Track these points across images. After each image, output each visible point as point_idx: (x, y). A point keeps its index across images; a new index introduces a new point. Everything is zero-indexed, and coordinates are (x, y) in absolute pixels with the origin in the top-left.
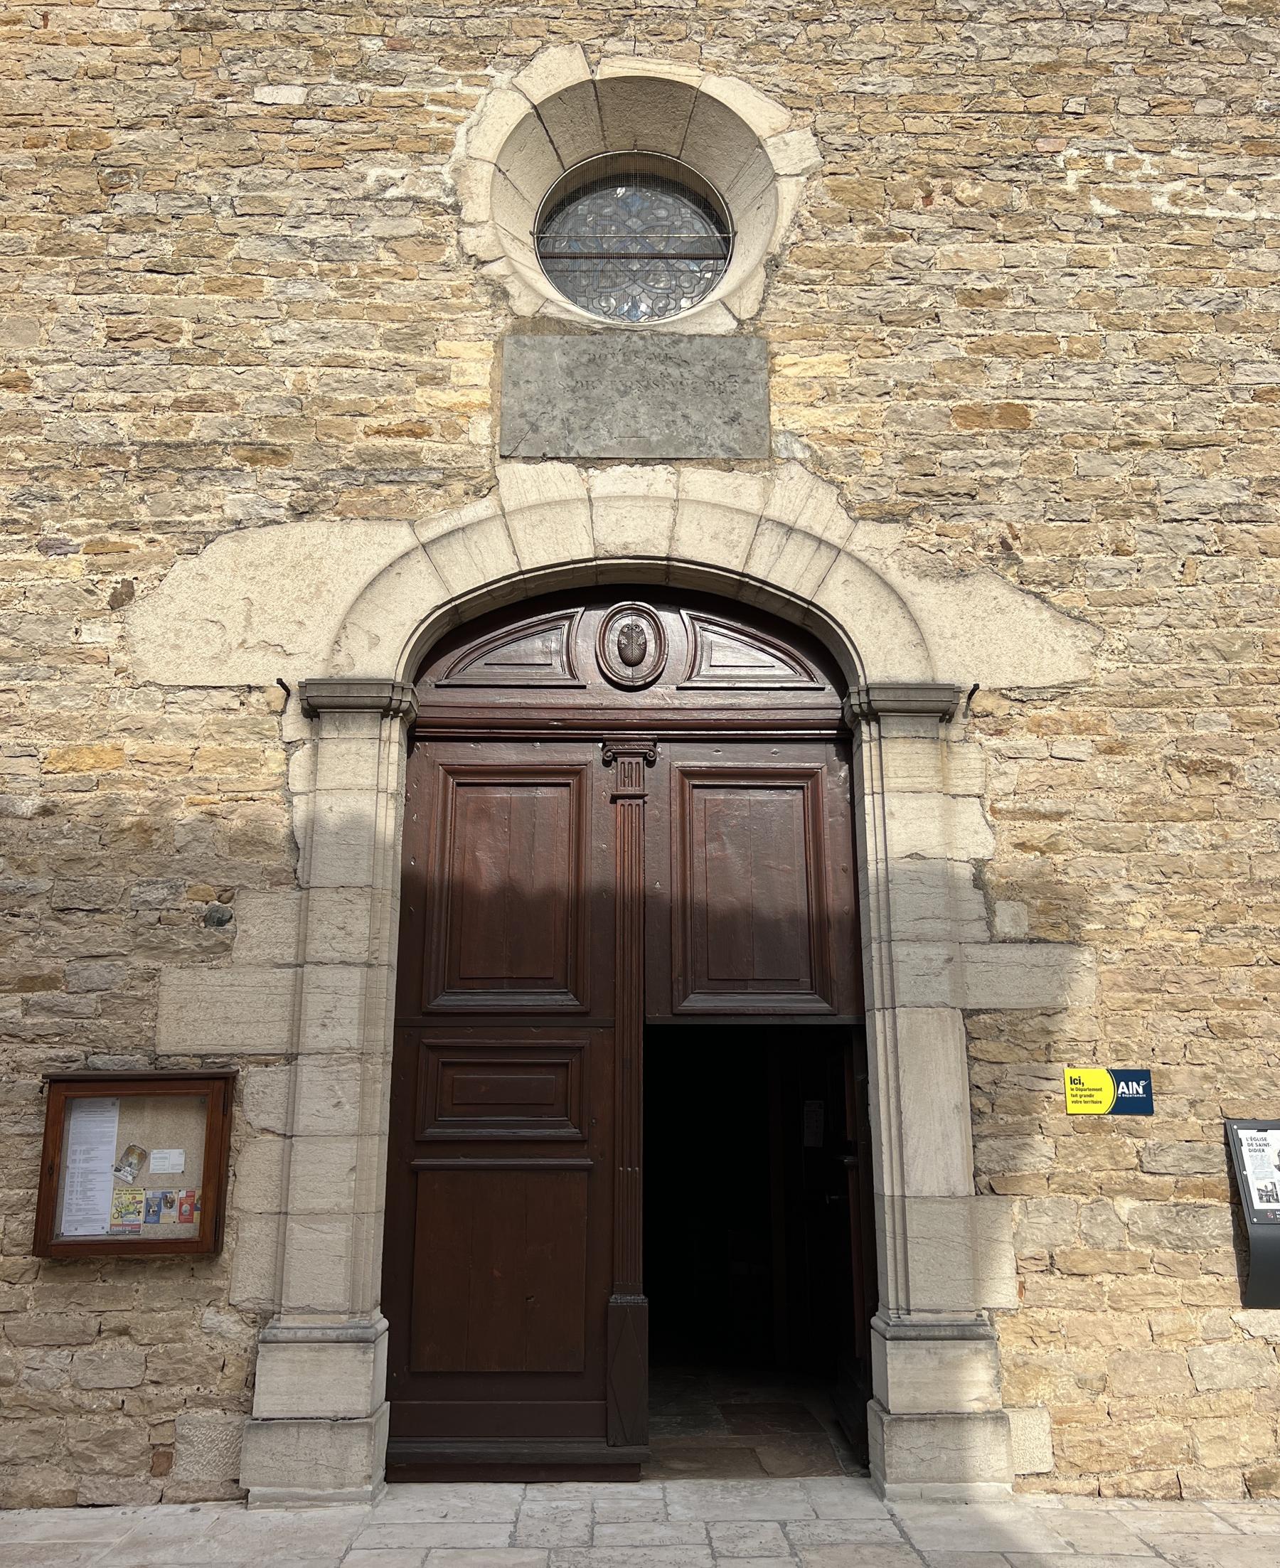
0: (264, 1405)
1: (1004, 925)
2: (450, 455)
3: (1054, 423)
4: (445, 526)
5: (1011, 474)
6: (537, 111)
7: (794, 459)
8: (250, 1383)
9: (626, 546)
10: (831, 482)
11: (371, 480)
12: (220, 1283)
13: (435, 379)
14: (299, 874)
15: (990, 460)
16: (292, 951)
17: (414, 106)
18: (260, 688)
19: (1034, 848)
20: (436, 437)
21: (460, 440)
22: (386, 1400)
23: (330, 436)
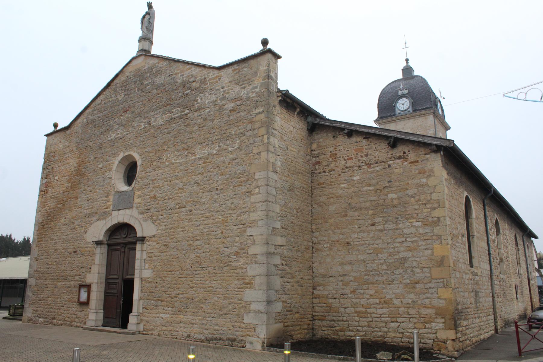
0: (89, 318)
1: (146, 267)
3: (158, 198)
6: (119, 162)
13: (108, 201)
17: (109, 165)
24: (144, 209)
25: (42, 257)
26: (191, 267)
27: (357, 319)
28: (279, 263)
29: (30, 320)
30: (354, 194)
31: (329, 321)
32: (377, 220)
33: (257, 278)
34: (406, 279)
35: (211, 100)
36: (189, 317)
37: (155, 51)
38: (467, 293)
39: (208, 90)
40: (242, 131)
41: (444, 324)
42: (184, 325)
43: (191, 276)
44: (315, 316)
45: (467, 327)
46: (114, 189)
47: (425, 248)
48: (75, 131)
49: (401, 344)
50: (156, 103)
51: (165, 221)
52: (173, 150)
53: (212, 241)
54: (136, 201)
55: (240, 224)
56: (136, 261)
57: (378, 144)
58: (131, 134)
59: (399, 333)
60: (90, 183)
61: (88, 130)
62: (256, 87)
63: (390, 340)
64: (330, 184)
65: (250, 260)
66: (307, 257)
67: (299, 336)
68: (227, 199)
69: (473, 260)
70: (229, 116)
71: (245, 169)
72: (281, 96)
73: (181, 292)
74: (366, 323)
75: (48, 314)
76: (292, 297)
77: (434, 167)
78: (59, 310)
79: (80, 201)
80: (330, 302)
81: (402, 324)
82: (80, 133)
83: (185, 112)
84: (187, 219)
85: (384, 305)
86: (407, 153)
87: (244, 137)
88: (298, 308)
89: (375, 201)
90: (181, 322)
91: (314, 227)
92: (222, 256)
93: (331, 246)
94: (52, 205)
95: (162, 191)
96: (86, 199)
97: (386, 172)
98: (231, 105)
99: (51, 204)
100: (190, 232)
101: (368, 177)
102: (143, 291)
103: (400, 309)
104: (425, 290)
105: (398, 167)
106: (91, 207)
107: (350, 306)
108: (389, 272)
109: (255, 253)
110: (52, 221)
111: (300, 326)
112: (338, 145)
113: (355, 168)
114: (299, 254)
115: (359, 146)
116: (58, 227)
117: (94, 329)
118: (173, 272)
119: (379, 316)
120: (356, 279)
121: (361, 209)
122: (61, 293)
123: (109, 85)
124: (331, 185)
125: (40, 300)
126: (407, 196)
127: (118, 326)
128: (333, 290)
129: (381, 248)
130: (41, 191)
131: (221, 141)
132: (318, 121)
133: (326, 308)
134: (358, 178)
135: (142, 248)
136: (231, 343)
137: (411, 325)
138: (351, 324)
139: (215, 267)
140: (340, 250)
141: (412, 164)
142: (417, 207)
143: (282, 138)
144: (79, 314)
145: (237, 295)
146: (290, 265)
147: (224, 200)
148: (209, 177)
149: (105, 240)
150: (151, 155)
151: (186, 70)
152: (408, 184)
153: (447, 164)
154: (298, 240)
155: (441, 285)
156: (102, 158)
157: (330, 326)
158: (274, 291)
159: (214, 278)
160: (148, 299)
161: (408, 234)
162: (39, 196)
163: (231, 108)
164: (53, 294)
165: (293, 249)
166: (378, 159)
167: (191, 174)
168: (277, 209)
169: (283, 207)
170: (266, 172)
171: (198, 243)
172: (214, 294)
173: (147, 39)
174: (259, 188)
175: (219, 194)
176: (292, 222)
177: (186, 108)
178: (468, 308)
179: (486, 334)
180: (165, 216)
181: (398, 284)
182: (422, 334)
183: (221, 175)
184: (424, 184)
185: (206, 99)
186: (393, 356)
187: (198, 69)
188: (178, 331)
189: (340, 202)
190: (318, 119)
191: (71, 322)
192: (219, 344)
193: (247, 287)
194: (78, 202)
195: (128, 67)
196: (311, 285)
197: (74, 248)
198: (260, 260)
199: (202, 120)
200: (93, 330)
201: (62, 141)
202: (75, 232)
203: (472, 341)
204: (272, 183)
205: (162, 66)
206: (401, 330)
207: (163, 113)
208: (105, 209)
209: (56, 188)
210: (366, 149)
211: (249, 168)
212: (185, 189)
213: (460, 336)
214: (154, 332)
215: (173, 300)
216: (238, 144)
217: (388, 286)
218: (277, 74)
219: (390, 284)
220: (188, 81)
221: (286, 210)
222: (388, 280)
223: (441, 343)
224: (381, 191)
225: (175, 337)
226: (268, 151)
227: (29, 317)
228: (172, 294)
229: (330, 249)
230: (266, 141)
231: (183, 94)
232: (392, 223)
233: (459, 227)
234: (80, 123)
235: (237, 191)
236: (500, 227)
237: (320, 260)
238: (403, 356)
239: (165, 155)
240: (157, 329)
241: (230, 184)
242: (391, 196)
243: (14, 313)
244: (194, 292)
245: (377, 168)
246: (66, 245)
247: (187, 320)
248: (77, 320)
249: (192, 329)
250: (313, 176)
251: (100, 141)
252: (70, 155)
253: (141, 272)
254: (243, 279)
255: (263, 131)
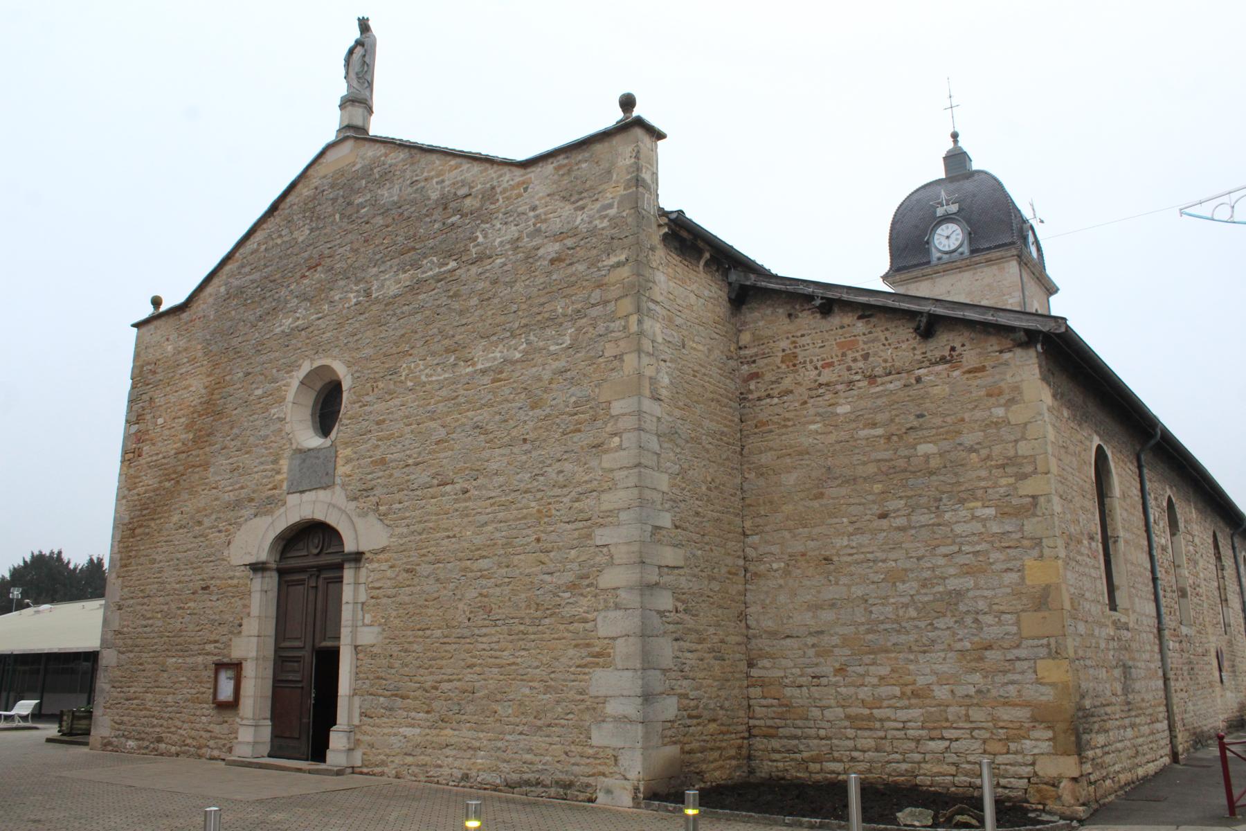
0: (240, 739)
1: (366, 621)
6: (302, 383)
13: (278, 473)
17: (279, 389)
24: (359, 488)
25: (131, 602)
26: (469, 619)
27: (850, 733)
28: (670, 607)
29: (106, 745)
30: (838, 447)
31: (786, 737)
32: (892, 505)
33: (619, 641)
34: (961, 640)
35: (508, 237)
36: (465, 733)
37: (377, 127)
38: (1104, 670)
39: (501, 215)
40: (579, 306)
41: (1051, 743)
42: (453, 753)
43: (468, 641)
44: (755, 727)
45: (1107, 749)
46: (291, 444)
47: (1005, 567)
48: (201, 314)
49: (953, 789)
50: (382, 248)
51: (407, 514)
52: (424, 353)
53: (516, 559)
54: (341, 470)
55: (579, 518)
56: (344, 607)
57: (894, 330)
58: (328, 318)
59: (948, 764)
60: (235, 431)
61: (229, 312)
62: (610, 206)
63: (928, 781)
64: (783, 423)
65: (602, 601)
66: (734, 593)
67: (717, 774)
68: (549, 462)
69: (1118, 594)
70: (550, 273)
71: (587, 393)
72: (666, 224)
73: (446, 677)
74: (872, 743)
75: (147, 730)
76: (701, 685)
77: (1022, 381)
78: (170, 721)
79: (215, 473)
80: (789, 694)
81: (954, 745)
82: (212, 317)
83: (449, 267)
84: (457, 510)
85: (913, 701)
86: (959, 349)
87: (584, 320)
88: (714, 710)
89: (886, 460)
90: (447, 745)
91: (748, 524)
92: (538, 592)
93: (788, 565)
94: (150, 483)
95: (400, 446)
96: (228, 467)
97: (911, 393)
98: (552, 249)
99: (150, 480)
100: (465, 540)
101: (869, 405)
103: (950, 709)
104: (1006, 664)
105: (938, 382)
106: (239, 485)
107: (833, 702)
108: (922, 624)
109: (614, 586)
110: (153, 519)
111: (719, 752)
112: (799, 334)
113: (839, 387)
114: (715, 586)
115: (847, 335)
116: (165, 533)
117: (250, 763)
118: (428, 632)
119: (901, 725)
120: (845, 641)
121: (854, 480)
122: (175, 683)
123: (274, 207)
124: (786, 426)
125: (127, 700)
126: (960, 448)
127: (305, 757)
128: (795, 666)
129: (903, 570)
130: (125, 452)
131: (531, 330)
132: (752, 279)
133: (780, 710)
134: (847, 408)
135: (356, 577)
136: (561, 791)
137: (977, 745)
138: (837, 746)
139: (522, 618)
140: (810, 574)
141: (972, 375)
142: (984, 473)
143: (671, 320)
144: (217, 729)
145: (573, 681)
146: (694, 612)
147: (541, 466)
148: (507, 413)
149: (272, 560)
150: (372, 365)
151: (450, 171)
152: (963, 420)
153: (1053, 374)
154: (713, 555)
155: (1044, 651)
156: (262, 374)
157: (788, 751)
158: (658, 672)
159: (521, 643)
160: (371, 694)
161: (966, 536)
162: (122, 462)
163: (554, 255)
164: (157, 684)
165: (700, 573)
166: (893, 366)
167: (464, 407)
168: (663, 482)
169: (675, 479)
170: (636, 398)
171: (483, 563)
172: (522, 680)
173: (360, 102)
174: (621, 437)
175: (530, 452)
176: (697, 514)
177: (450, 256)
178: (1108, 705)
179: (1150, 765)
180: (406, 504)
181: (943, 650)
182: (1002, 767)
183: (532, 408)
184: (1000, 420)
185: (498, 235)
186: (935, 817)
187: (476, 168)
188: (440, 767)
189: (808, 465)
190: (752, 277)
191: (199, 748)
192: (535, 794)
193: (598, 664)
194: (210, 475)
195: (316, 167)
196: (743, 657)
197: (203, 580)
198: (624, 602)
199: (488, 283)
200: (249, 765)
201: (171, 338)
202: (204, 544)
203: (1119, 781)
204: (650, 424)
205: (394, 161)
206: (954, 758)
207: (398, 270)
208: (270, 489)
209: (160, 444)
210: (865, 343)
211: (597, 390)
212: (452, 442)
213: (1090, 771)
214: (386, 769)
215: (428, 694)
216: (571, 336)
217: (920, 656)
218: (657, 174)
219: (925, 652)
220: (455, 194)
221: (684, 485)
222: (920, 644)
223: (1045, 786)
224: (900, 437)
225: (436, 779)
226: (639, 351)
227: (105, 738)
228: (426, 682)
229: (787, 573)
230: (634, 328)
231: (444, 224)
232: (926, 511)
233: (1082, 518)
234: (210, 295)
235: (570, 443)
236: (1179, 516)
237: (762, 597)
238: (958, 818)
239: (404, 365)
240: (392, 762)
241: (555, 427)
242: (923, 449)
243: (72, 728)
244: (476, 677)
245: (891, 386)
246: (184, 572)
247: (462, 740)
248: (211, 743)
249: (473, 761)
250: (744, 407)
251: (257, 335)
252: (190, 368)
253: (354, 633)
254: (588, 645)
255: (627, 305)
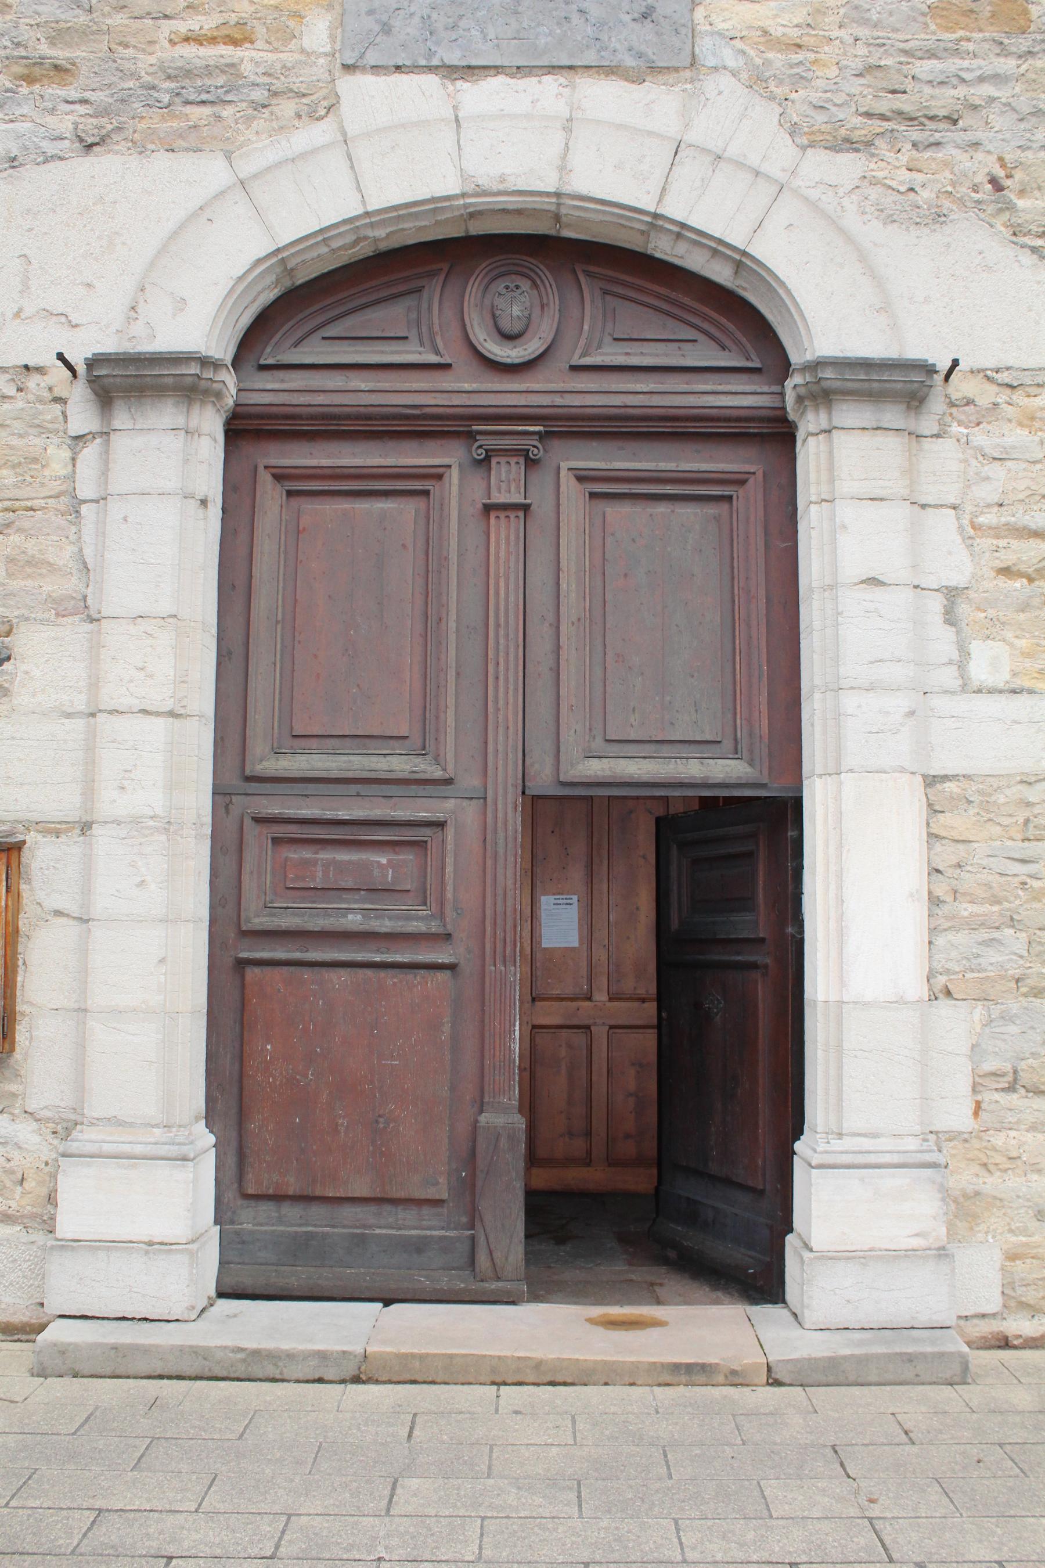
0: (67, 1226)
1: (980, 671)
2: (278, 66)
4: (272, 156)
5: (1003, 93)
7: (725, 68)
8: (51, 1199)
9: (502, 179)
10: (772, 98)
11: (177, 100)
12: (13, 1087)
14: (89, 602)
15: (978, 73)
16: (83, 697)
18: (40, 370)
19: (1021, 575)
20: (259, 44)
21: (293, 45)
22: (216, 1223)
23: (126, 46)
24: (868, 103)
102: (966, 909)
